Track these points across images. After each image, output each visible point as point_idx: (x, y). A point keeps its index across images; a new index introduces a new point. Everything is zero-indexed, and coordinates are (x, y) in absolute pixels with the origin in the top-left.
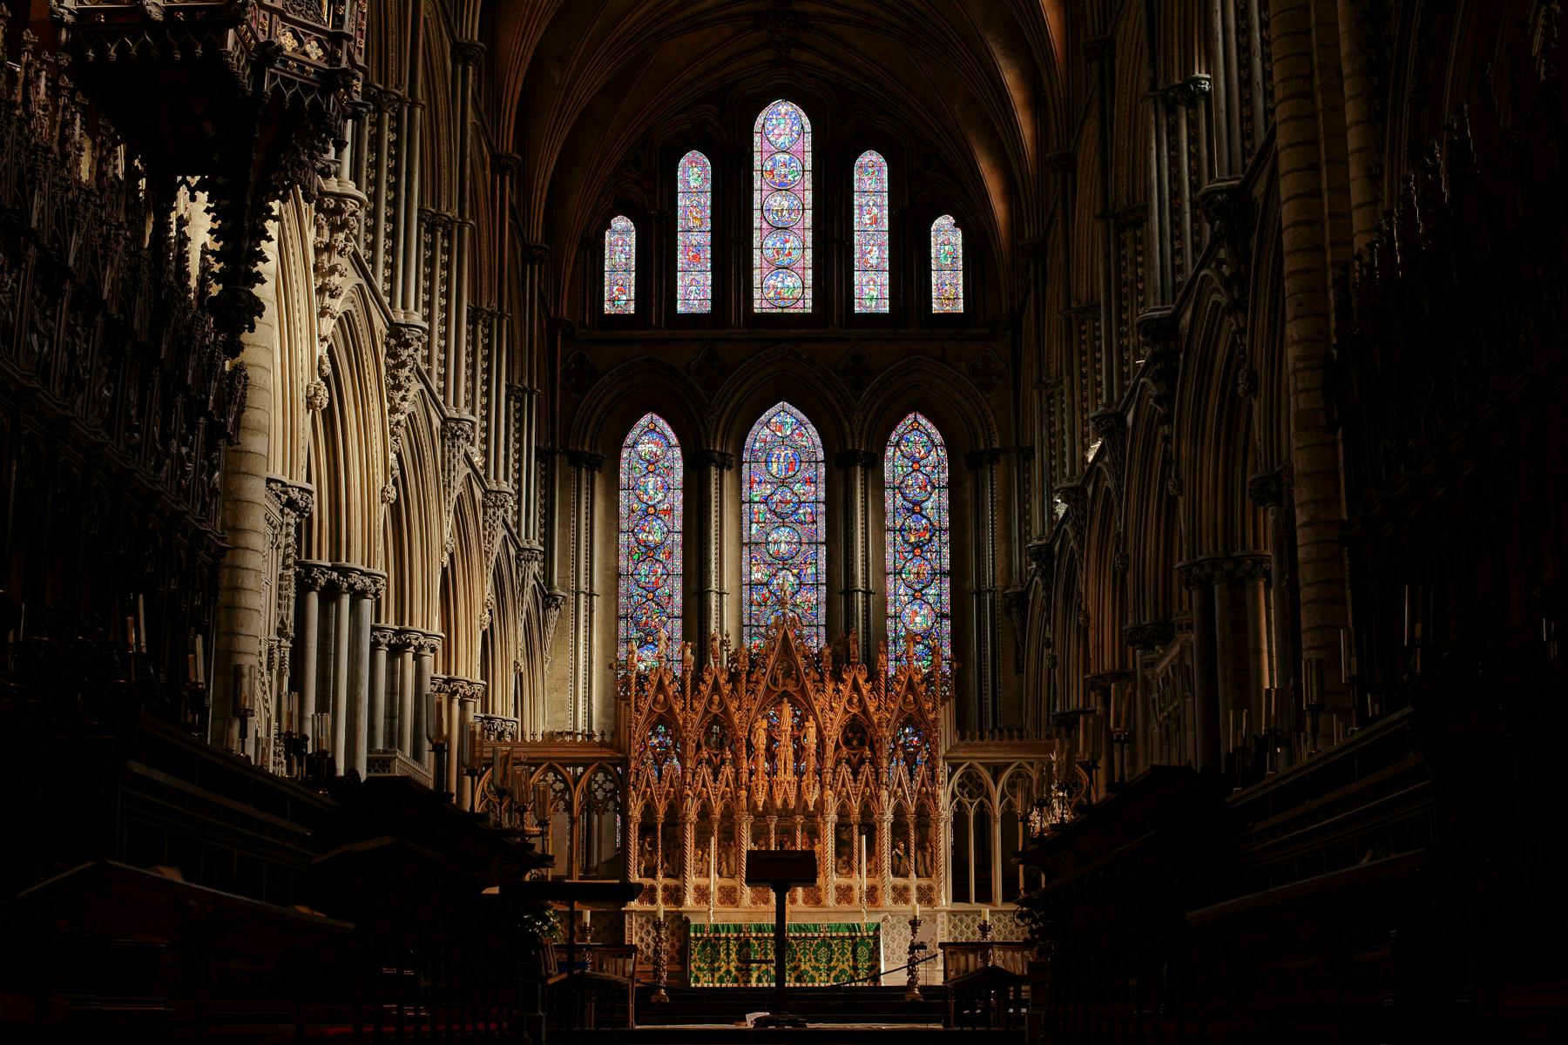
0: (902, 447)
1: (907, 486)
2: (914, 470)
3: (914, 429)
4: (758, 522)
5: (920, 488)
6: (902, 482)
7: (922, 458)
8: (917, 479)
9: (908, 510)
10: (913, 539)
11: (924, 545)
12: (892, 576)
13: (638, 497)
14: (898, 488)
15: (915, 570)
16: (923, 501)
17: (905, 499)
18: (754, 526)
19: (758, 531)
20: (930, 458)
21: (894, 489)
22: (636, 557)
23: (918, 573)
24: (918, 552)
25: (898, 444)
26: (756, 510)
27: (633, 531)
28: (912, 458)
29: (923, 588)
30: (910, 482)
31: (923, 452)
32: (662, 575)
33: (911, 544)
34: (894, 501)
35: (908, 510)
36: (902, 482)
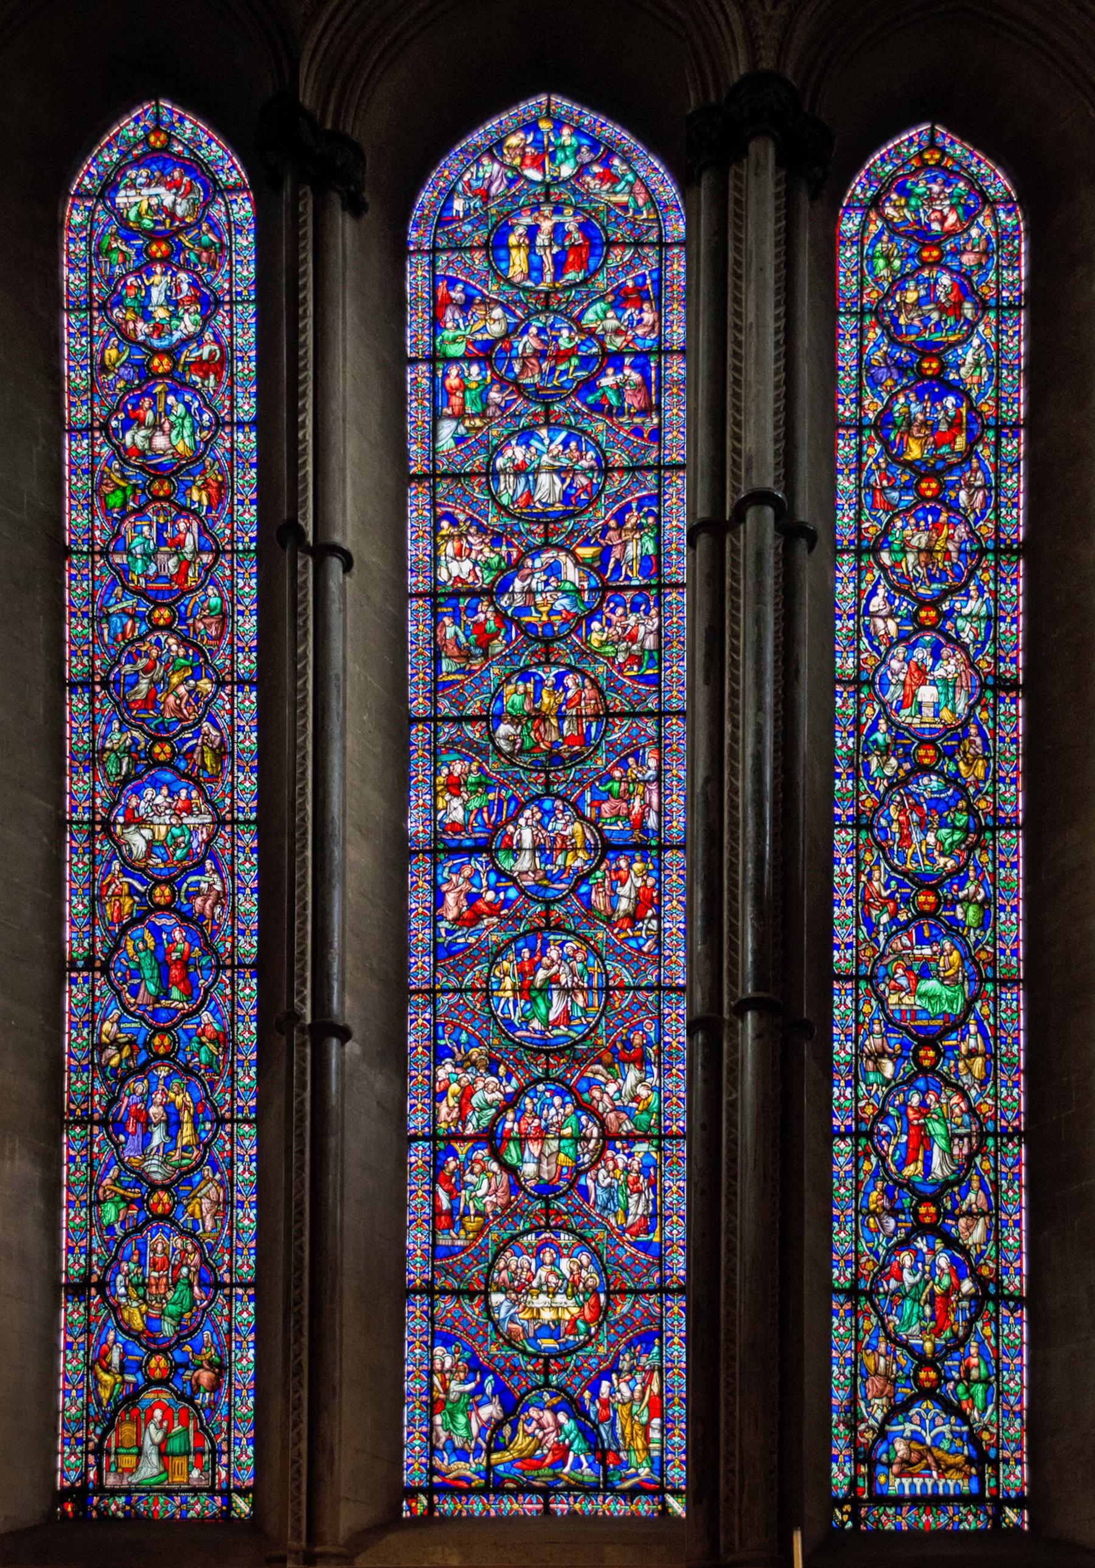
0: (889, 211)
1: (901, 306)
2: (925, 264)
3: (924, 166)
4: (460, 416)
5: (941, 309)
6: (888, 296)
7: (950, 234)
8: (932, 287)
9: (901, 368)
10: (915, 452)
11: (950, 468)
12: (847, 561)
13: (119, 328)
14: (877, 313)
15: (920, 540)
16: (952, 345)
17: (893, 342)
18: (447, 429)
19: (459, 440)
20: (974, 232)
21: (861, 315)
22: (115, 500)
23: (929, 550)
24: (929, 487)
25: (876, 203)
26: (453, 381)
27: (105, 427)
28: (922, 235)
29: (944, 595)
30: (911, 297)
31: (952, 218)
32: (199, 551)
33: (909, 465)
34: (861, 348)
35: (901, 368)
36: (888, 296)
